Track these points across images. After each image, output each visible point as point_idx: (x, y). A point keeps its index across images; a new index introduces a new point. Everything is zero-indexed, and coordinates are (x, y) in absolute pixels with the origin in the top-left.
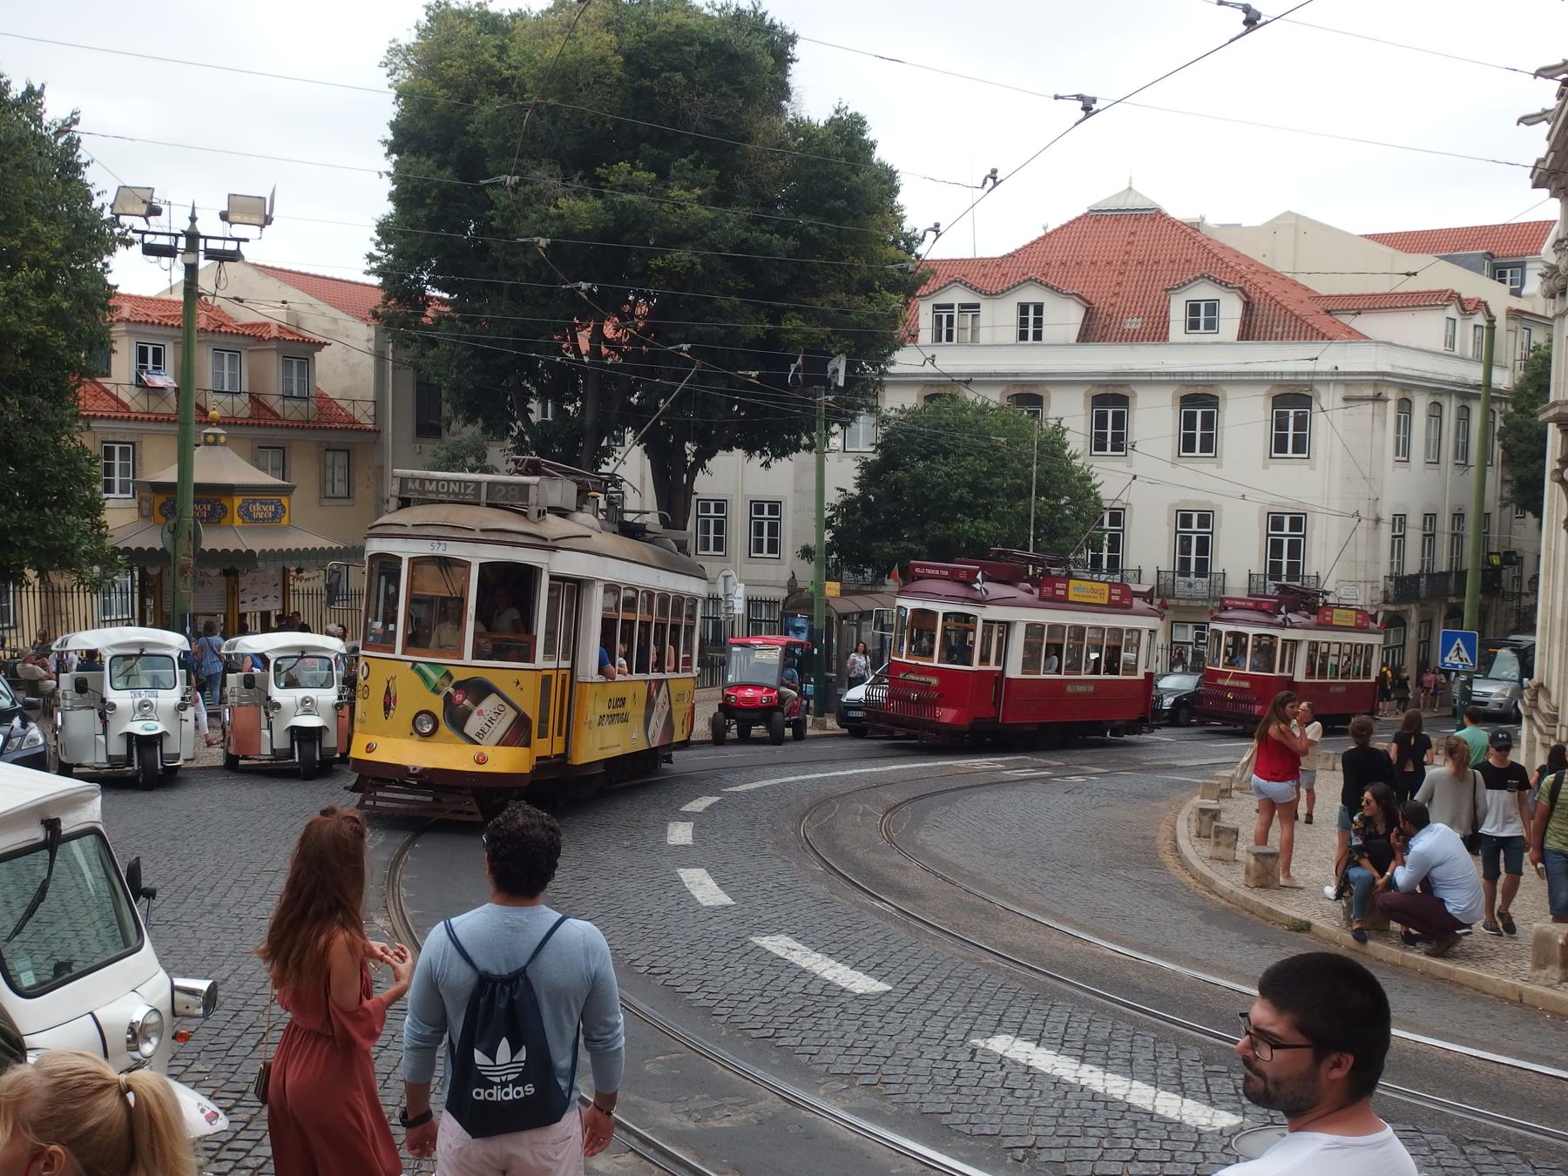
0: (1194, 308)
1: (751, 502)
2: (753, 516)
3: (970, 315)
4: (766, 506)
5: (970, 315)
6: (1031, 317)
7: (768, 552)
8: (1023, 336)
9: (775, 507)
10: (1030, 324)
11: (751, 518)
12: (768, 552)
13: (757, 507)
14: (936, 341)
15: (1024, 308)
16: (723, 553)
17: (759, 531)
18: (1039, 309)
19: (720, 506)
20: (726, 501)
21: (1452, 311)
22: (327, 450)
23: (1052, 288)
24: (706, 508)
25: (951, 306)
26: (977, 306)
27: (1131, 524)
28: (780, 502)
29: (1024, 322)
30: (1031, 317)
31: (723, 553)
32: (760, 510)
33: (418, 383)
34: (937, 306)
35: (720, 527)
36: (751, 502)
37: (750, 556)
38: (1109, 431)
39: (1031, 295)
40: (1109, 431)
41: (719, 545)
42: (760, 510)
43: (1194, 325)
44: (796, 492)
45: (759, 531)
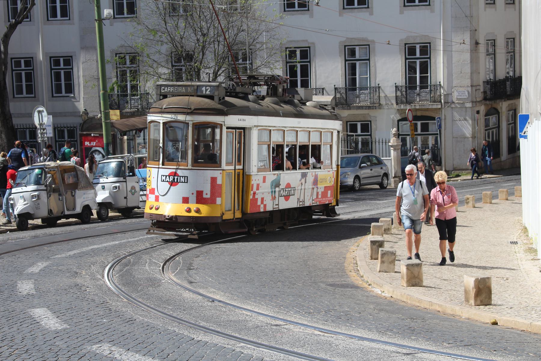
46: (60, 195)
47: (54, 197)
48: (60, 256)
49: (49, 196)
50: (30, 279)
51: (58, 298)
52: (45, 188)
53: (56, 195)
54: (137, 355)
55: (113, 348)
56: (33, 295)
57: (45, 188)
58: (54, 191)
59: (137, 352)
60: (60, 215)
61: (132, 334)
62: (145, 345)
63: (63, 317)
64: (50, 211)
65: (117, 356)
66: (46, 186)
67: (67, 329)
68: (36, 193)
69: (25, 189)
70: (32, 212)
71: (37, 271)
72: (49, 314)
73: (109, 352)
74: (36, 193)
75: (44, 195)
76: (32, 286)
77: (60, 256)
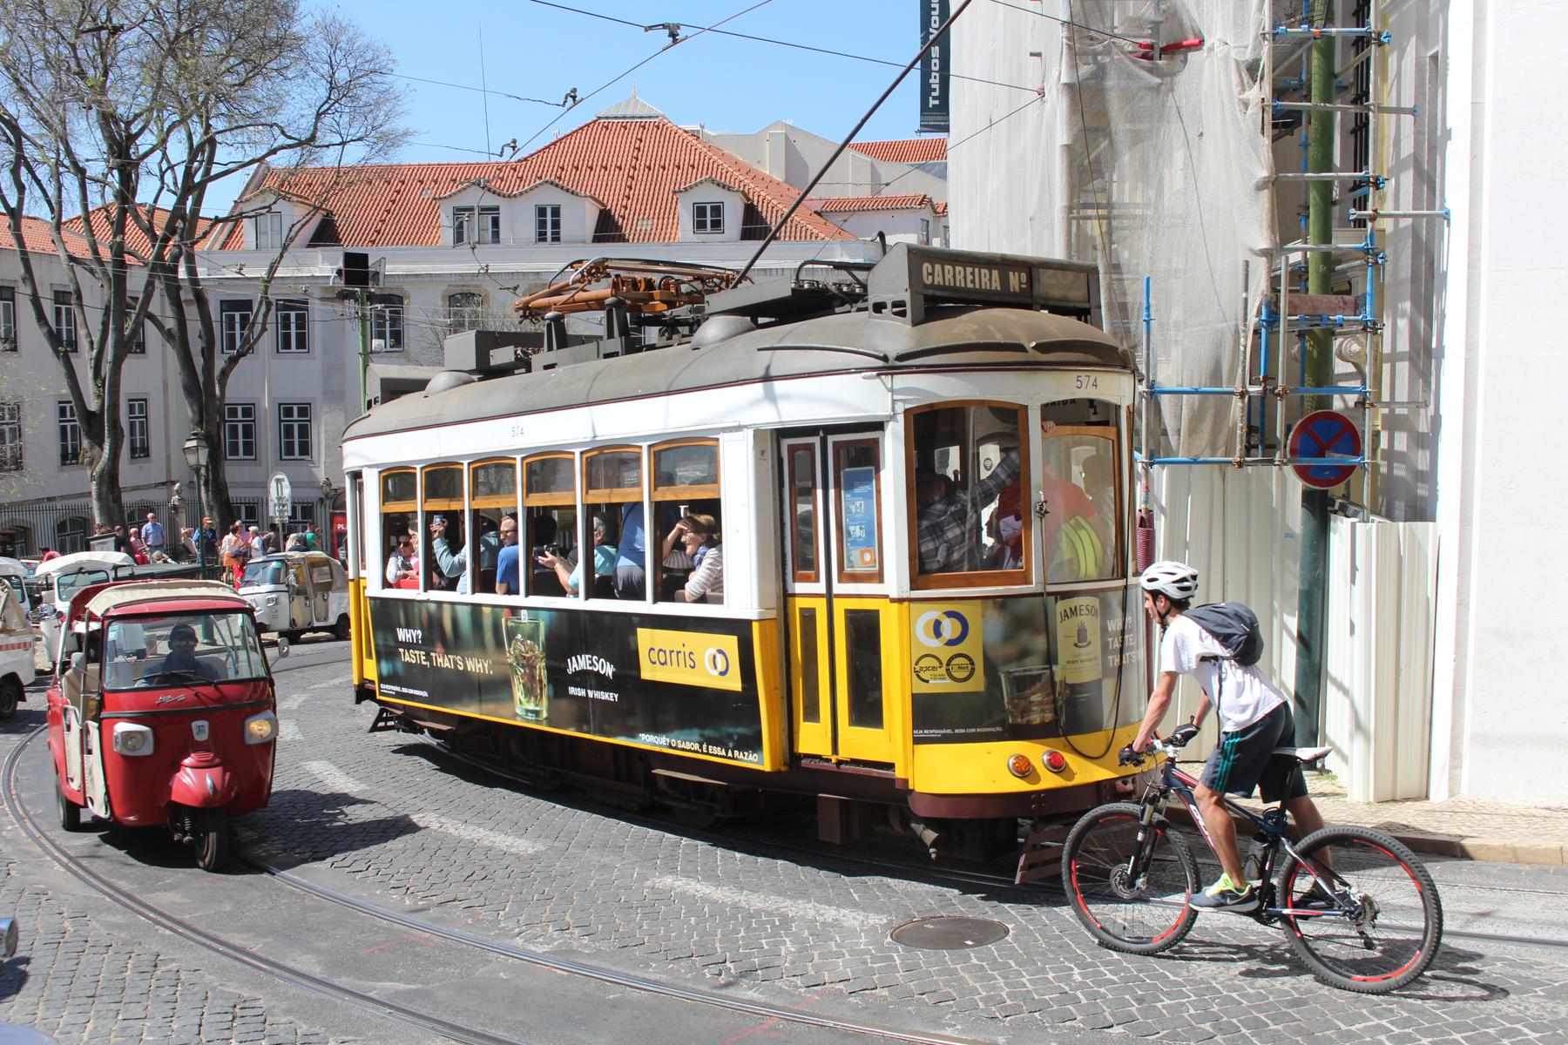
0: (700, 211)
1: (280, 405)
3: (490, 217)
4: (295, 408)
5: (490, 217)
6: (549, 219)
7: (244, 454)
8: (542, 237)
10: (548, 225)
11: (281, 421)
12: (244, 454)
15: (542, 212)
16: (253, 457)
18: (556, 212)
19: (248, 412)
21: (926, 213)
23: (567, 190)
24: (233, 412)
25: (471, 209)
26: (497, 209)
28: (310, 404)
29: (542, 224)
30: (549, 219)
31: (253, 457)
32: (289, 412)
34: (459, 211)
35: (248, 431)
36: (280, 405)
37: (281, 459)
39: (550, 197)
41: (249, 449)
42: (289, 412)
43: (700, 225)
44: (325, 393)
45: (289, 431)
46: (307, 598)
47: (299, 600)
48: (320, 686)
49: (291, 600)
50: (289, 718)
51: (339, 746)
52: (286, 589)
53: (302, 598)
54: (481, 830)
55: (443, 820)
56: (300, 741)
57: (286, 589)
58: (299, 592)
59: (479, 825)
60: (306, 627)
61: (464, 799)
62: (488, 816)
63: (356, 774)
64: (293, 622)
65: (452, 830)
66: (288, 586)
67: (367, 791)
68: (274, 596)
69: (256, 589)
70: (266, 623)
71: (295, 707)
72: (333, 769)
73: (439, 825)
74: (274, 596)
75: (284, 598)
76: (296, 728)
77: (320, 686)
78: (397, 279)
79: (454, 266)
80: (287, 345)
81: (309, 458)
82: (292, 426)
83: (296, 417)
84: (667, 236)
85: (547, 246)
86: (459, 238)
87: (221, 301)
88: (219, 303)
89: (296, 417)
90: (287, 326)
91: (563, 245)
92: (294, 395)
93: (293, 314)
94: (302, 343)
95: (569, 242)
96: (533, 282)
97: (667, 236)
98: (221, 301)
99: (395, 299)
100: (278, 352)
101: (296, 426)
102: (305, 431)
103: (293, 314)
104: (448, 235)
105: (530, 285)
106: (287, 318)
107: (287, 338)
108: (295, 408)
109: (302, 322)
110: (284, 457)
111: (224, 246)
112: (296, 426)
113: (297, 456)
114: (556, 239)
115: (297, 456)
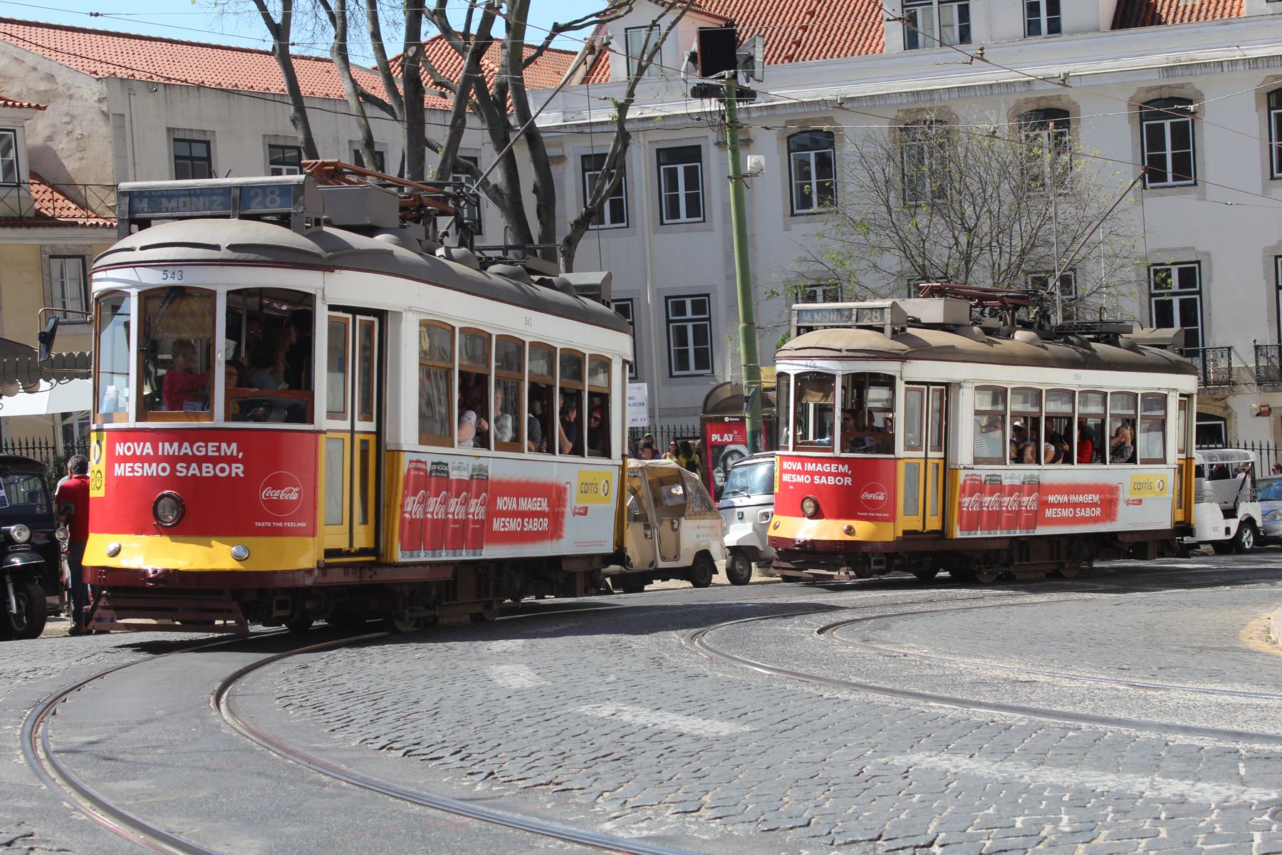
1: (667, 298)
2: (671, 318)
4: (688, 302)
8: (1032, 29)
9: (701, 304)
11: (669, 321)
13: (675, 305)
14: (910, 48)
17: (682, 339)
20: (631, 300)
22: (51, 257)
27: (1210, 280)
28: (708, 295)
32: (680, 308)
33: (177, 157)
36: (667, 298)
37: (671, 376)
38: (1169, 152)
40: (1169, 152)
78: (824, 108)
79: (897, 83)
80: (674, 213)
81: (708, 371)
82: (685, 328)
83: (689, 315)
84: (1227, 11)
85: (1043, 43)
86: (912, 42)
87: (583, 157)
88: (580, 159)
89: (689, 315)
90: (673, 185)
91: (1064, 37)
92: (685, 281)
93: (681, 169)
94: (695, 208)
95: (1072, 33)
96: (1023, 97)
97: (1227, 11)
98: (583, 157)
99: (819, 137)
100: (662, 223)
101: (690, 326)
102: (702, 334)
103: (681, 169)
104: (894, 35)
105: (1018, 101)
106: (672, 175)
107: (674, 201)
108: (688, 302)
109: (693, 179)
110: (675, 373)
111: (585, 80)
112: (690, 326)
113: (692, 370)
114: (1055, 28)
115: (692, 370)
